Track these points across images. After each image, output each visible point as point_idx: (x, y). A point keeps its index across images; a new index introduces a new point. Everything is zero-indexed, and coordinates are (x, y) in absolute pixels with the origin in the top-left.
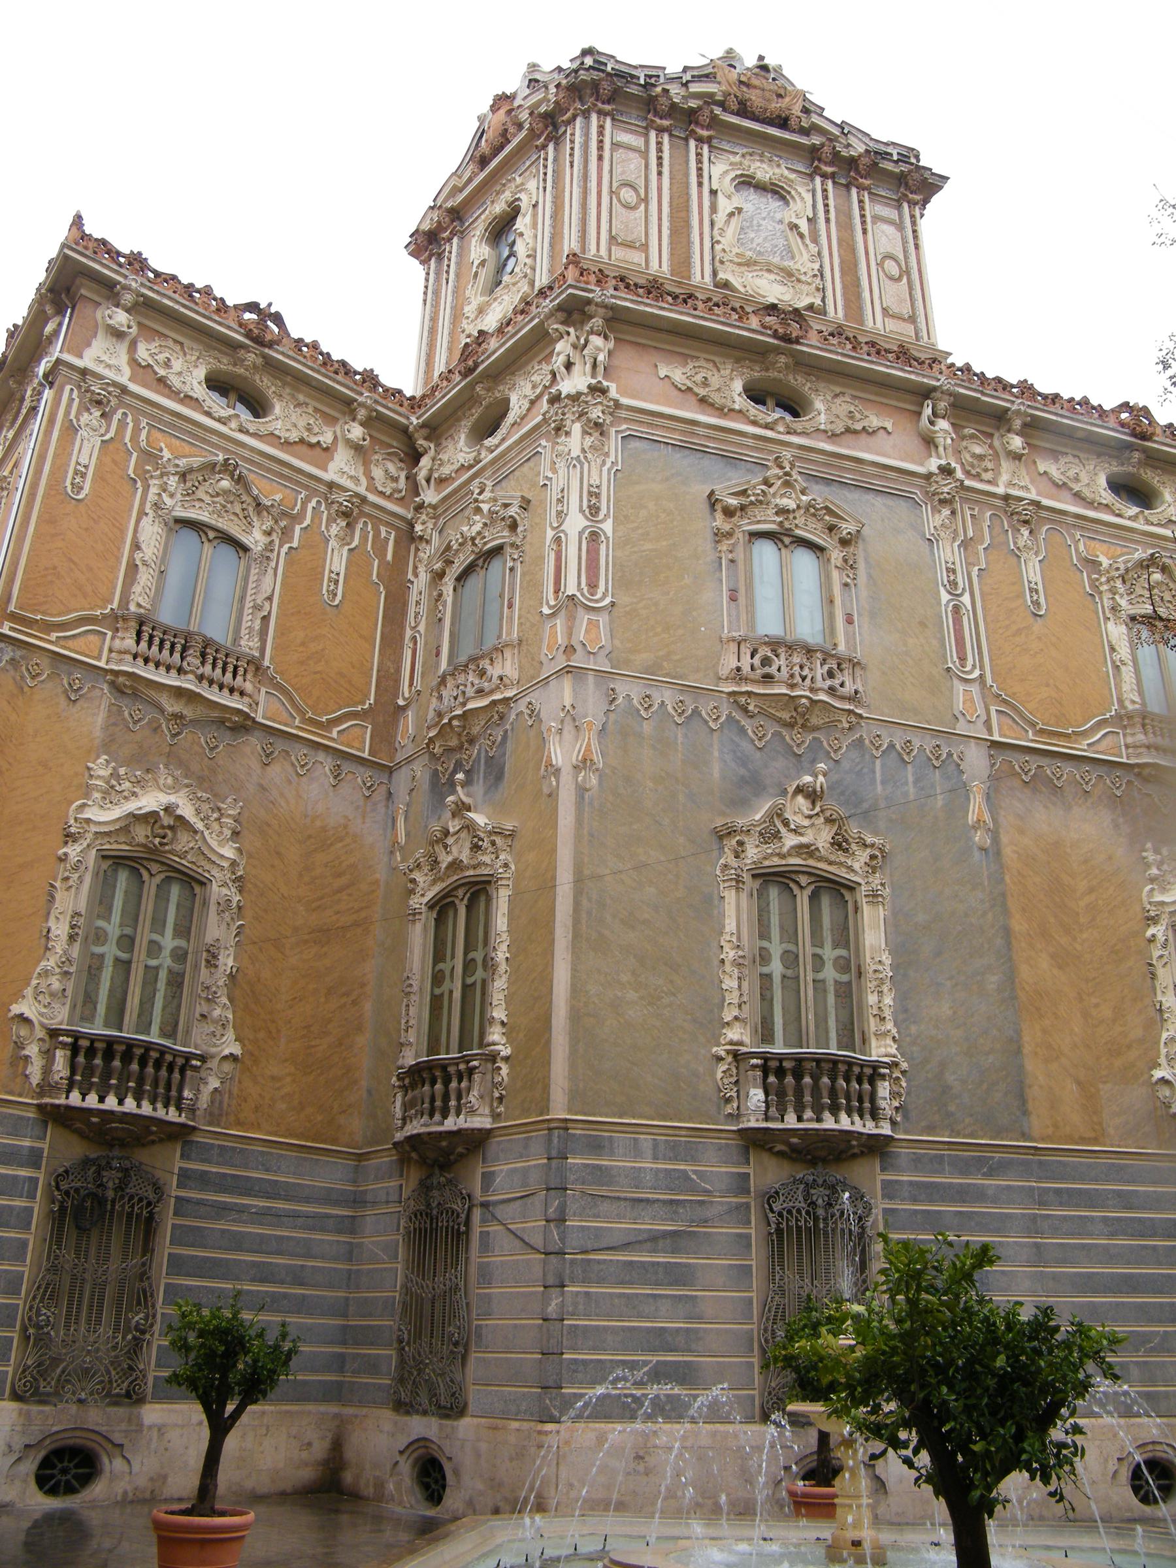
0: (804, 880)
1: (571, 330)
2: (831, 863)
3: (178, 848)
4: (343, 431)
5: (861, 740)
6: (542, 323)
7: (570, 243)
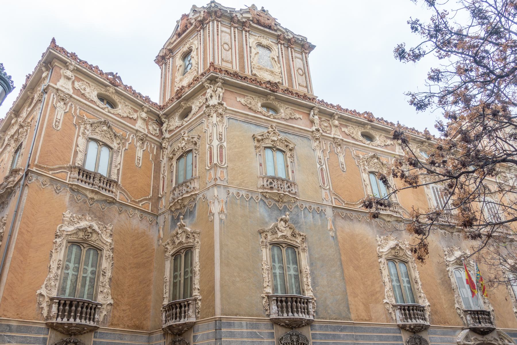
0: (284, 245)
1: (212, 86)
2: (291, 240)
3: (93, 239)
4: (140, 114)
5: (297, 206)
6: (203, 83)
7: (210, 60)
